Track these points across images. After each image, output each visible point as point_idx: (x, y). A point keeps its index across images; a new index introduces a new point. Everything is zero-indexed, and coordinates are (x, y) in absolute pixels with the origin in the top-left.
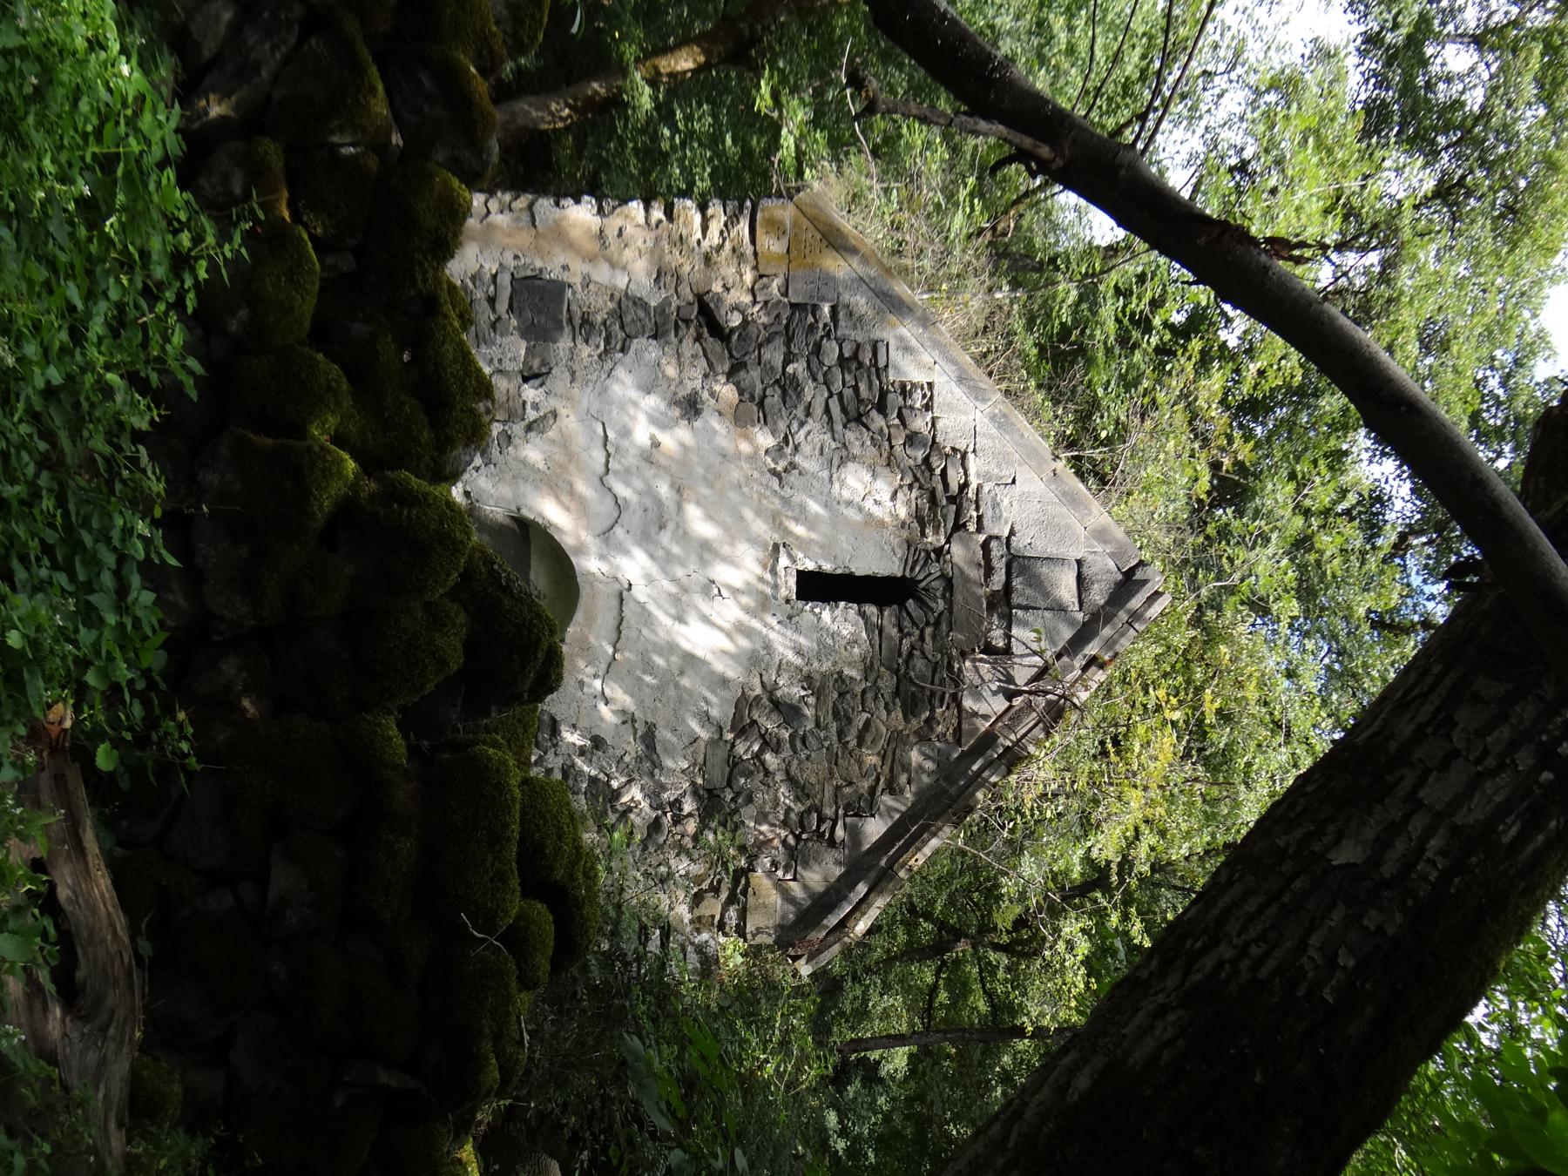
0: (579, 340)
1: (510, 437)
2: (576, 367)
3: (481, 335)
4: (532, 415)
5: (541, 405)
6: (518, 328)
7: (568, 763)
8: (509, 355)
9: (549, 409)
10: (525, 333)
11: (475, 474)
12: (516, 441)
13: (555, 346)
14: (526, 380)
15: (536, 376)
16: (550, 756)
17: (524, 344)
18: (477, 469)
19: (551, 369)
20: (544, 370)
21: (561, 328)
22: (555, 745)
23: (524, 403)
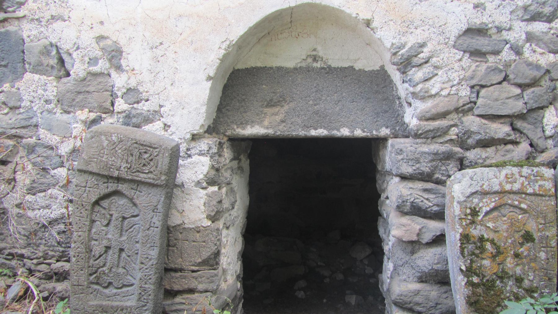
0: (20, 13)
1: (129, 90)
2: (48, 16)
3: (24, 123)
4: (102, 66)
5: (92, 55)
6: (13, 81)
7: (520, 13)
8: (40, 92)
9: (95, 45)
10: (18, 75)
11: (172, 129)
12: (133, 83)
13: (27, 40)
14: (68, 75)
15: (62, 61)
16: (511, 36)
17: (28, 76)
18: (166, 127)
19: (51, 45)
20: (54, 52)
21: (7, 33)
22: (499, 30)
23: (89, 73)
